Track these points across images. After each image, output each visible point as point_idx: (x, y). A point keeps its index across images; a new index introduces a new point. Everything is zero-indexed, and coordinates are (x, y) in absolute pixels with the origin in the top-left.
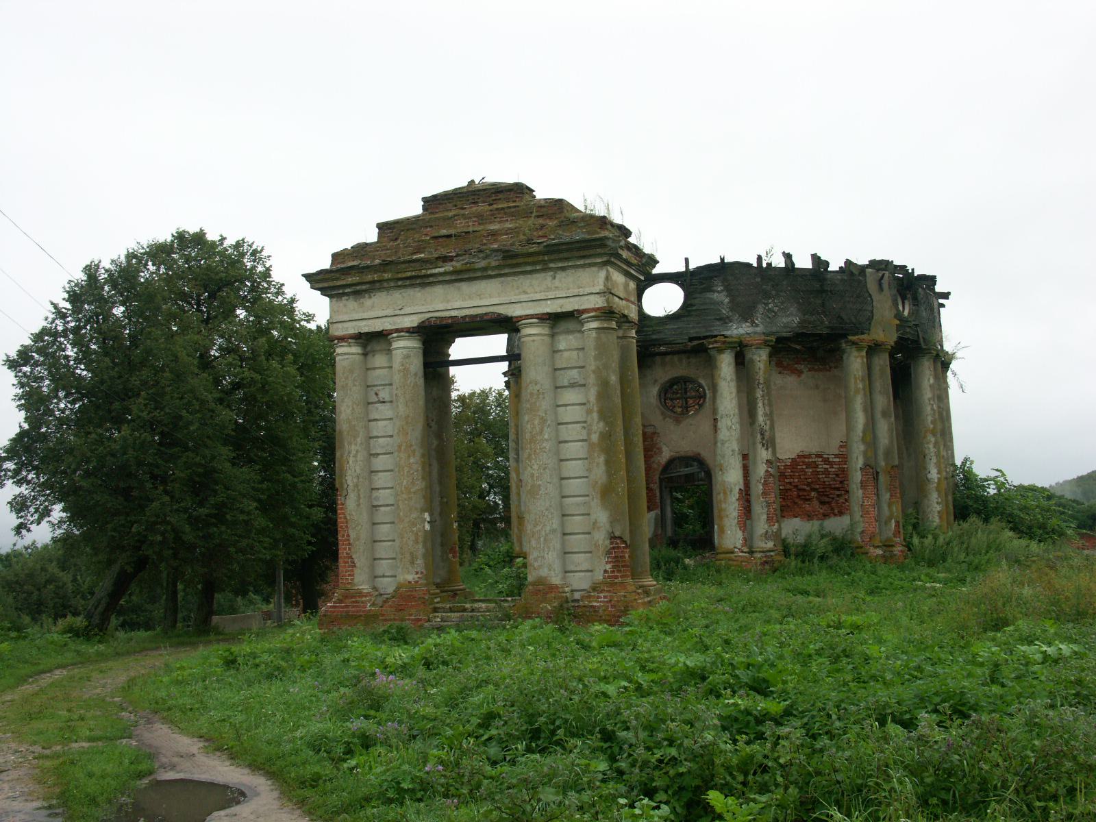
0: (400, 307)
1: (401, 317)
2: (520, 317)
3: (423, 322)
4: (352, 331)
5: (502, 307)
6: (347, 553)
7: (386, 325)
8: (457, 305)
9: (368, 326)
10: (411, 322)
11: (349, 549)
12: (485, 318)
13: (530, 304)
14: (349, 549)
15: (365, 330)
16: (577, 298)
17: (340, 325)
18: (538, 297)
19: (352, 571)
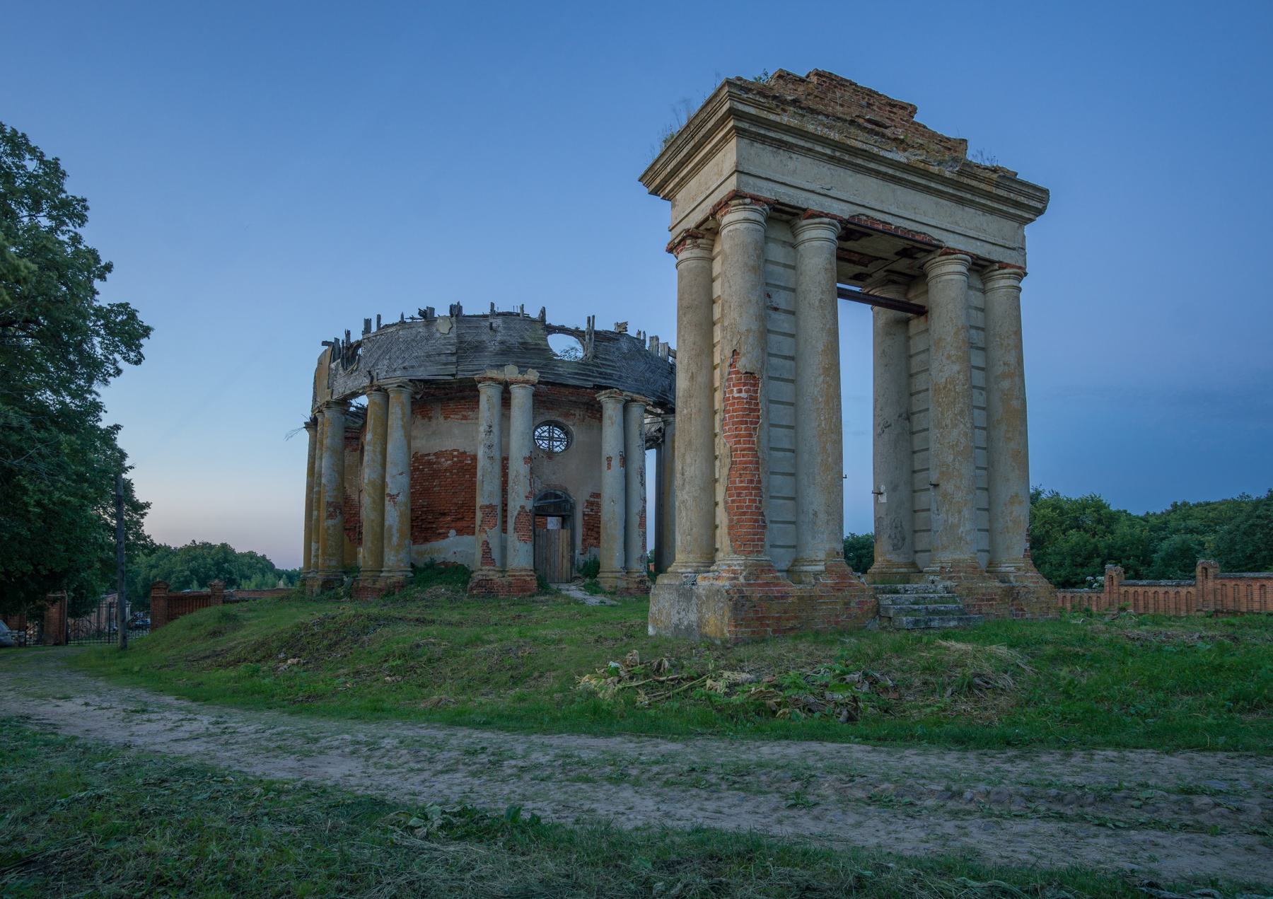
0: (829, 187)
1: (829, 200)
2: (954, 249)
3: (853, 217)
4: (767, 195)
5: (934, 230)
6: (756, 507)
7: (813, 203)
8: (894, 210)
9: (789, 196)
10: (844, 211)
11: (760, 502)
12: (917, 238)
13: (962, 238)
14: (760, 502)
15: (785, 200)
16: (1002, 249)
17: (751, 180)
18: (971, 233)
19: (762, 534)
